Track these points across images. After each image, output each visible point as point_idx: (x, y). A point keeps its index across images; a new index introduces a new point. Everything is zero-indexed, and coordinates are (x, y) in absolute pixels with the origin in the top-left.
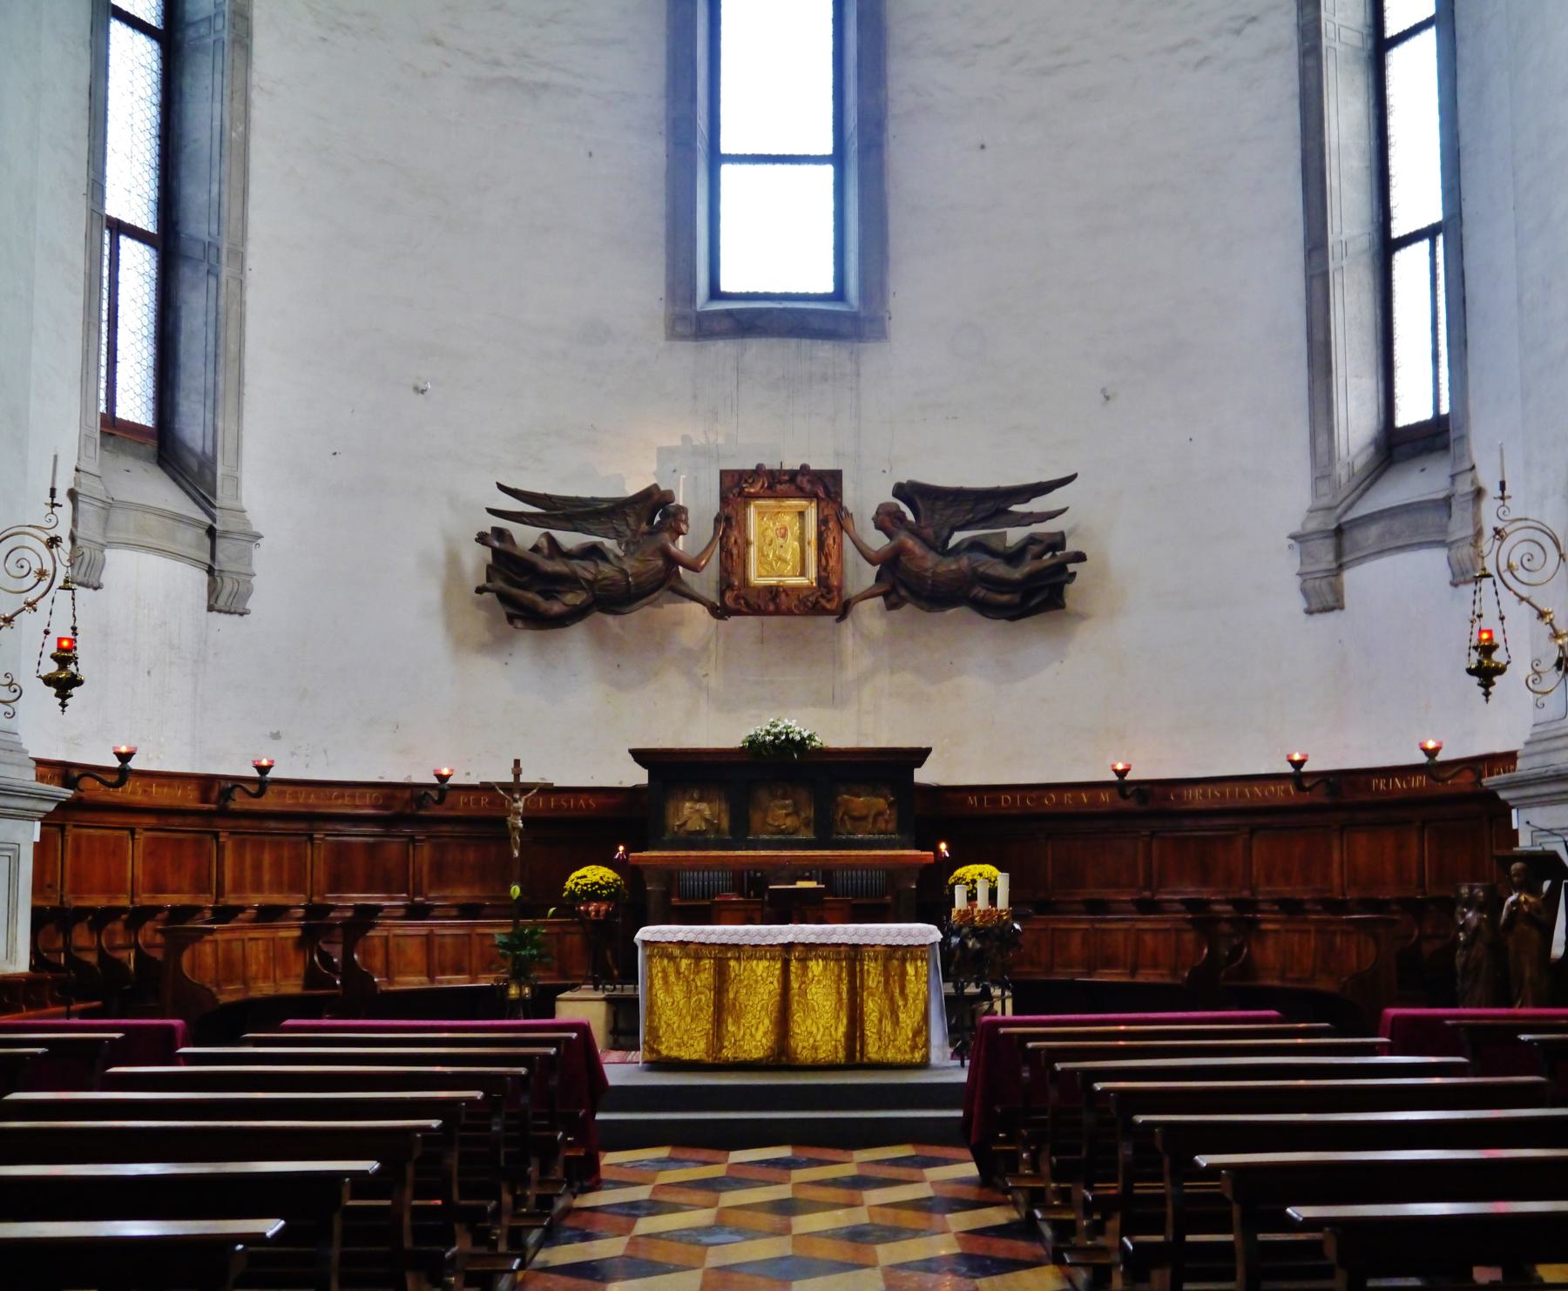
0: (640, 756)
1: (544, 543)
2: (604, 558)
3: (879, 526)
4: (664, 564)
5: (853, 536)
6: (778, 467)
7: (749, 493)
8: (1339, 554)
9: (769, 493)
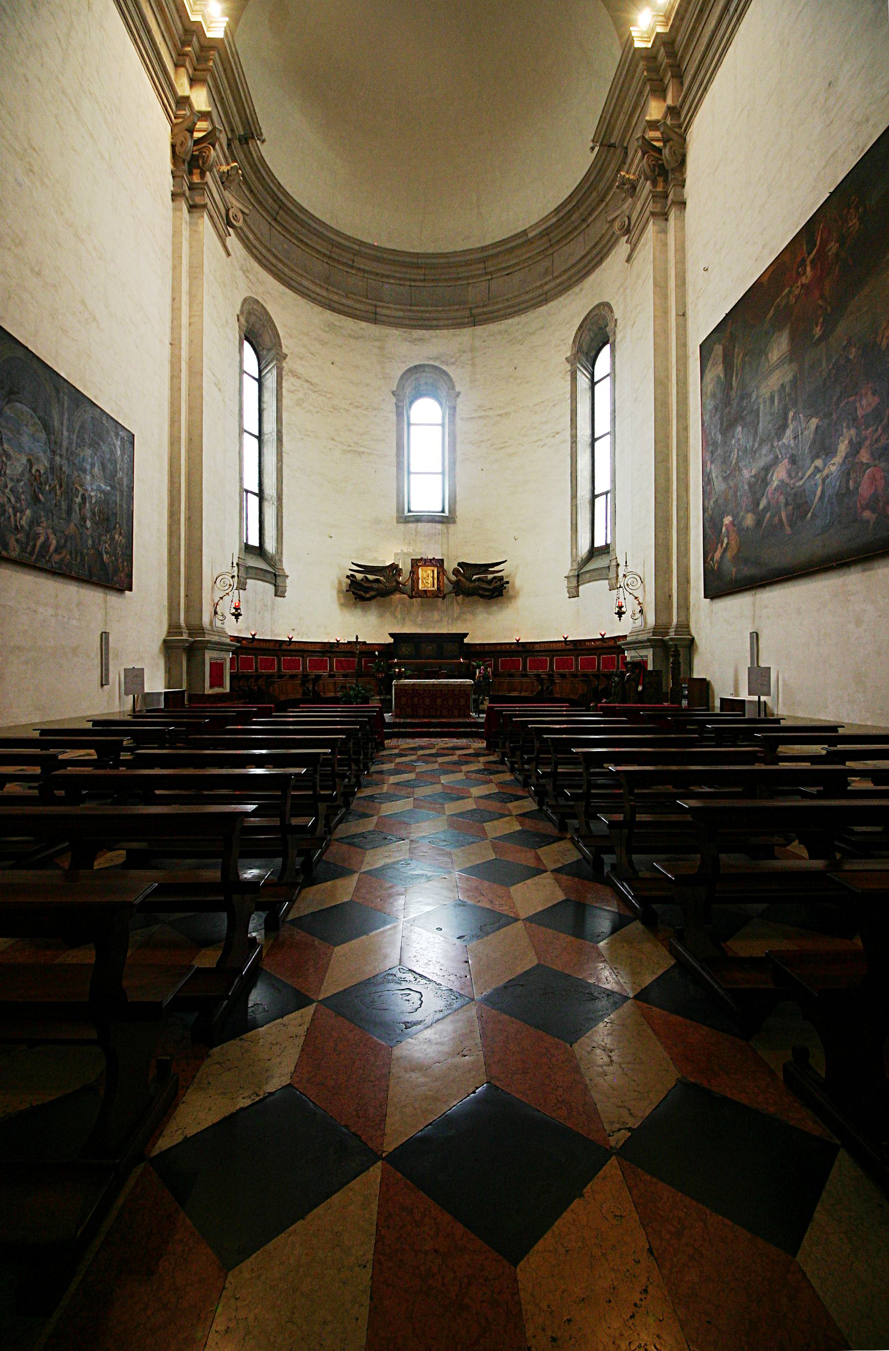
0: (392, 635)
3: (454, 574)
8: (578, 582)
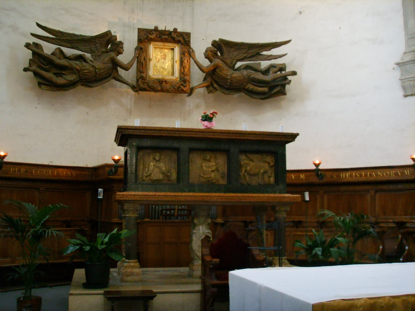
1: (58, 52)
3: (207, 57)
6: (164, 29)
7: (151, 38)
9: (159, 39)
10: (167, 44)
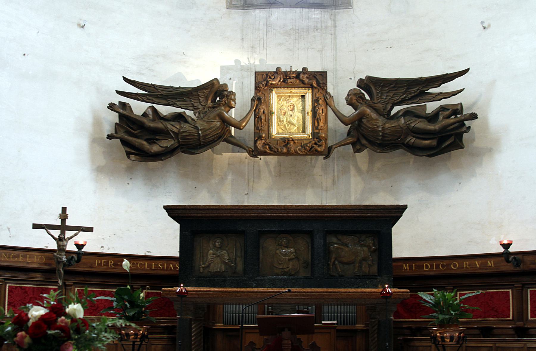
1: (150, 112)
2: (186, 121)
3: (349, 104)
4: (221, 124)
5: (334, 108)
7: (271, 84)
9: (283, 83)
10: (294, 90)
